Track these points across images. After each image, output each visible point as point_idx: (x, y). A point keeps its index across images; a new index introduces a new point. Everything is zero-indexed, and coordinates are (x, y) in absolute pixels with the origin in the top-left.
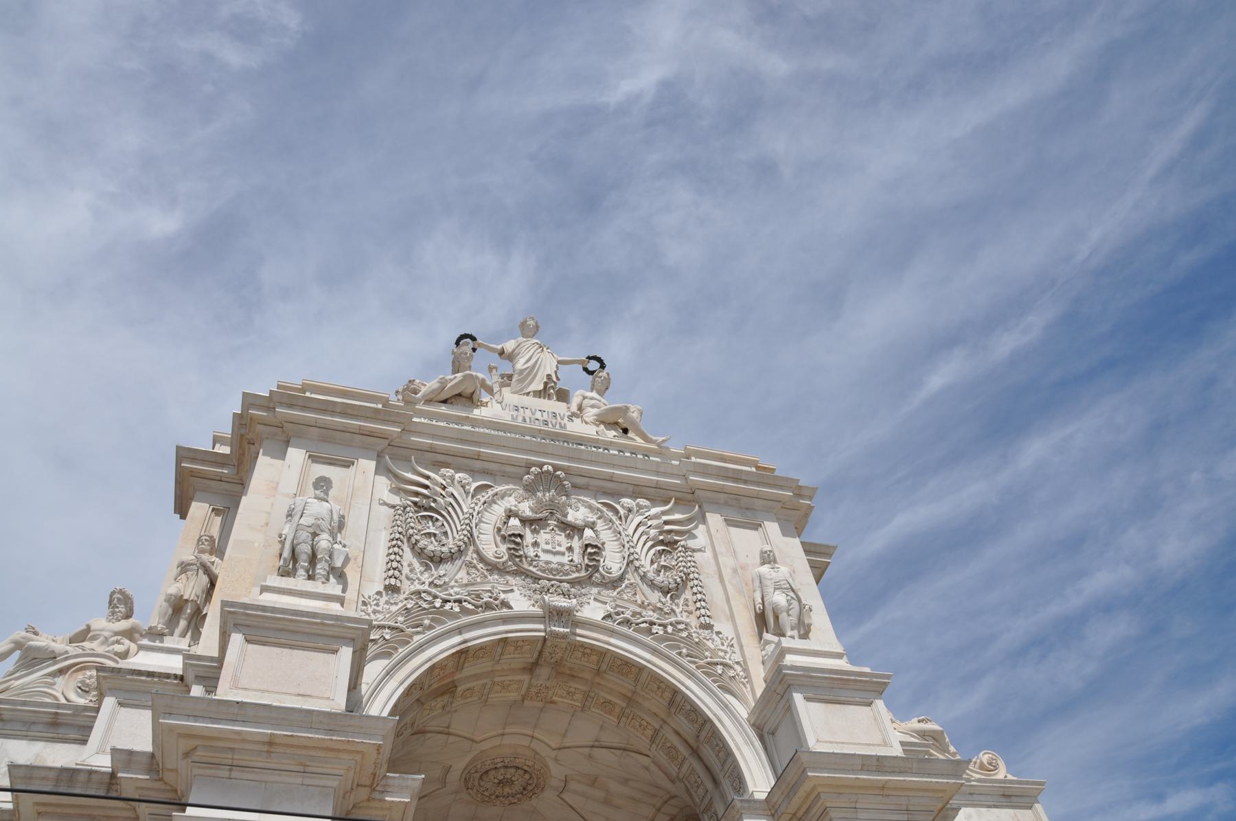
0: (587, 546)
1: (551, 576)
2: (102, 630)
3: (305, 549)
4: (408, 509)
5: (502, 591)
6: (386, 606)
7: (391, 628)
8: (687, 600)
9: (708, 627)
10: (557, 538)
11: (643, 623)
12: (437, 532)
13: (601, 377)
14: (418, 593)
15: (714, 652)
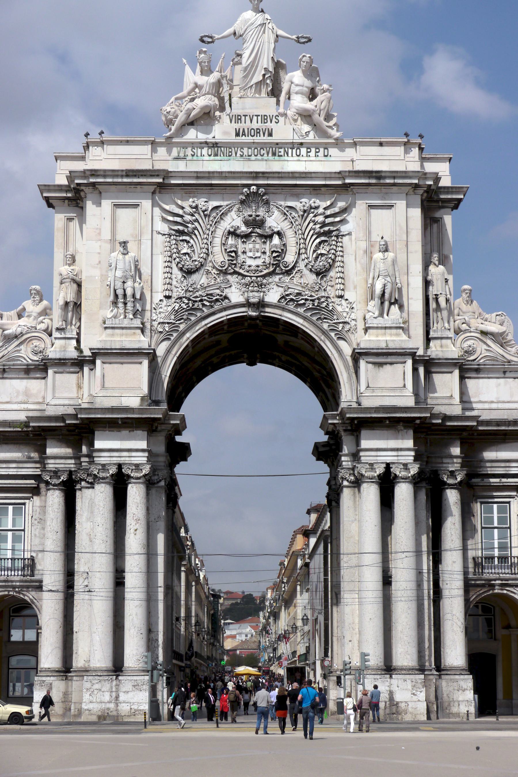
0: (273, 252)
1: (252, 275)
2: (32, 312)
3: (120, 292)
4: (172, 237)
5: (225, 288)
6: (165, 308)
7: (168, 323)
8: (332, 277)
9: (341, 297)
10: (257, 246)
11: (301, 300)
12: (189, 251)
13: (304, 62)
14: (181, 298)
15: (339, 315)
